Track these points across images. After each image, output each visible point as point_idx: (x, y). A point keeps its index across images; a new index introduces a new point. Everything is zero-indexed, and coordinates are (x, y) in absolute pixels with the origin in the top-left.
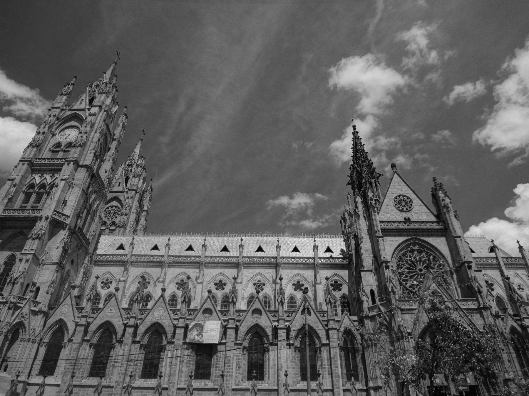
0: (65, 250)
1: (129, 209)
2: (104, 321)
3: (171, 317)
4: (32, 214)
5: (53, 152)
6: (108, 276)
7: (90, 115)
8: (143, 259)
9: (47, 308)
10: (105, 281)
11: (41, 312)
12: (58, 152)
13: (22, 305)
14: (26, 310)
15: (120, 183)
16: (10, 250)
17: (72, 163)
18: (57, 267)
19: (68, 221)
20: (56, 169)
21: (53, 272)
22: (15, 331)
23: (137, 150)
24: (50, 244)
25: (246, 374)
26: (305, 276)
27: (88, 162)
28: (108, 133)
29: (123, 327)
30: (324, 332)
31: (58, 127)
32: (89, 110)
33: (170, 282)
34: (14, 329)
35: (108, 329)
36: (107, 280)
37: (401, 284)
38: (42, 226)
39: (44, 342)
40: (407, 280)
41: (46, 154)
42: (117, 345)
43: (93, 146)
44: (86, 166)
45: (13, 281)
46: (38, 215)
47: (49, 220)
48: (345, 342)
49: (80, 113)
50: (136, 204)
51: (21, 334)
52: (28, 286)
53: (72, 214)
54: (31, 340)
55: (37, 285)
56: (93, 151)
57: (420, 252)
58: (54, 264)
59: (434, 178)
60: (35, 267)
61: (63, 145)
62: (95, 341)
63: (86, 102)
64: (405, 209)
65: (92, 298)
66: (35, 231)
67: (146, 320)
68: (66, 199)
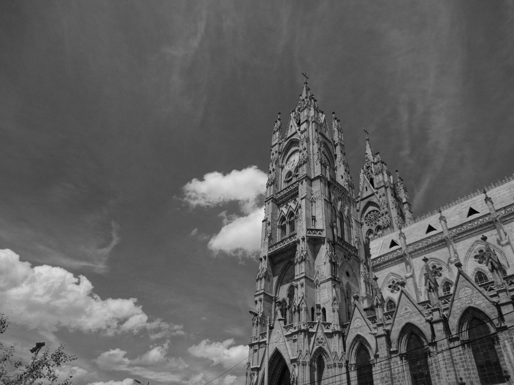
0: (333, 264)
1: (387, 207)
2: (403, 324)
3: (486, 294)
5: (288, 182)
6: (392, 277)
8: (421, 245)
9: (339, 327)
10: (391, 284)
11: (335, 332)
12: (291, 179)
13: (315, 331)
14: (320, 334)
15: (366, 187)
16: (288, 283)
17: (304, 180)
18: (332, 283)
19: (324, 235)
20: (294, 195)
21: (331, 289)
22: (318, 359)
23: (369, 151)
24: (317, 262)
27: (318, 173)
28: (327, 142)
29: (428, 325)
31: (283, 159)
32: (299, 130)
33: (466, 259)
34: (317, 357)
35: (412, 333)
36: (393, 282)
38: (302, 248)
39: (351, 364)
42: (431, 349)
43: (316, 157)
44: (318, 177)
45: (297, 309)
46: (296, 239)
47: (306, 240)
49: (294, 137)
50: (391, 199)
51: (325, 360)
52: (313, 310)
53: (325, 227)
54: (337, 365)
55: (322, 307)
56: (318, 162)
58: (328, 280)
60: (312, 289)
61: (293, 171)
62: (403, 350)
63: (295, 126)
65: (379, 302)
66: (298, 255)
67: (454, 309)
68: (314, 215)
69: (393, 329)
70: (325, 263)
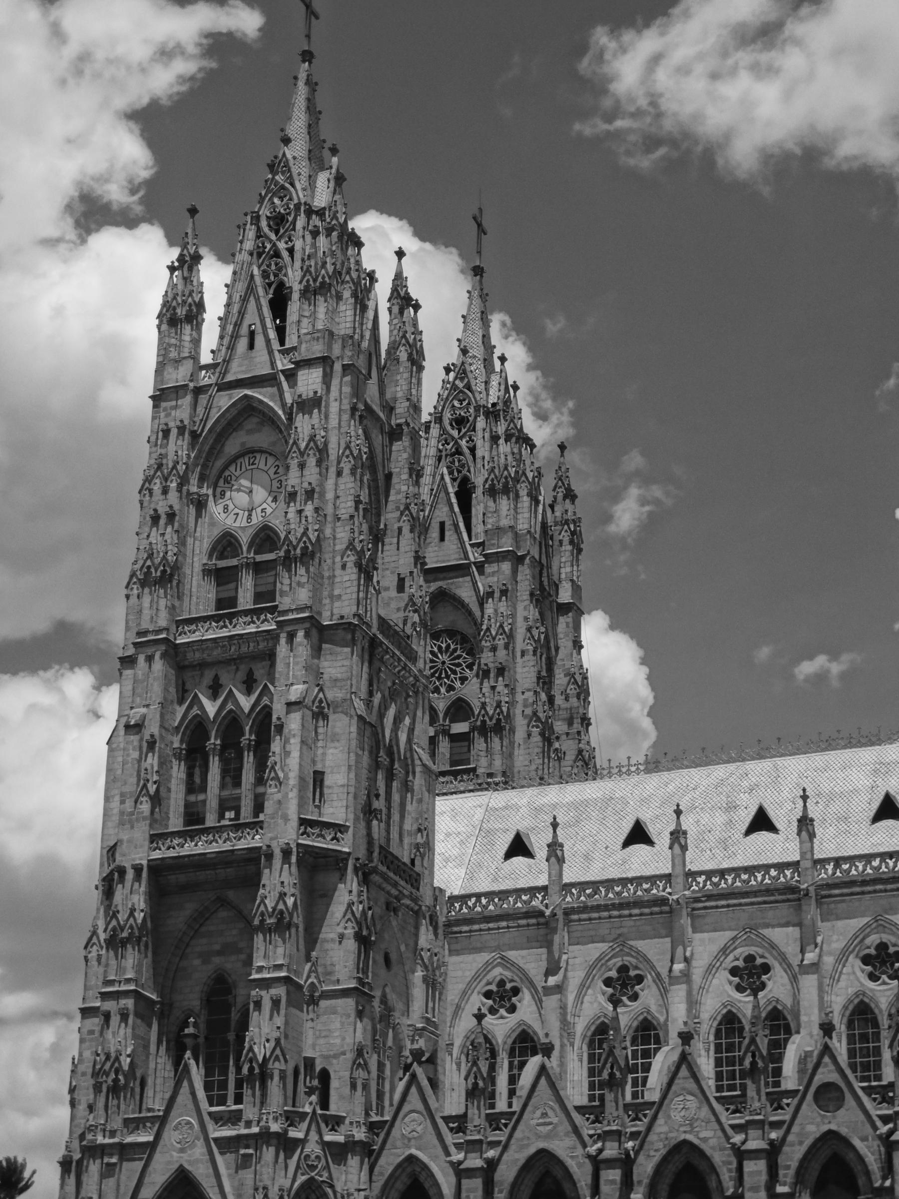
0: (363, 940)
1: (506, 646)
2: (532, 1150)
3: (723, 1120)
10: (493, 987)
13: (301, 1135)
15: (442, 525)
17: (301, 634)
18: (357, 1003)
21: (352, 1019)
29: (588, 1167)
32: (291, 376)
33: (710, 970)
38: (279, 884)
41: (200, 595)
47: (294, 859)
53: (351, 816)
56: (351, 559)
61: (244, 539)
63: (268, 341)
67: (652, 1137)
68: (319, 767)
69: (505, 1157)
70: (342, 937)
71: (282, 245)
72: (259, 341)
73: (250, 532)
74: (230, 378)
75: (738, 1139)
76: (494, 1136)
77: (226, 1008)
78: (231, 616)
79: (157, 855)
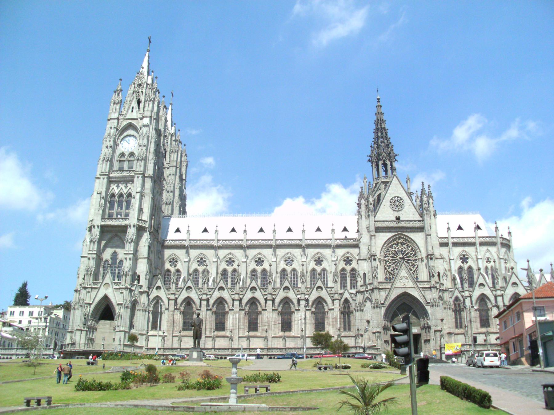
4: (124, 222)
7: (144, 126)
11: (145, 292)
12: (124, 161)
14: (136, 292)
16: (112, 247)
19: (147, 225)
25: (280, 328)
26: (324, 254)
29: (199, 300)
30: (331, 301)
36: (173, 259)
37: (385, 268)
38: (131, 232)
40: (390, 266)
41: (116, 166)
48: (345, 307)
49: (134, 122)
57: (403, 244)
58: (145, 258)
59: (423, 183)
61: (127, 154)
64: (397, 209)
71: (140, 91)
72: (134, 110)
73: (129, 153)
74: (127, 118)
75: (233, 297)
76: (177, 293)
77: (116, 259)
78: (123, 171)
79: (103, 223)
